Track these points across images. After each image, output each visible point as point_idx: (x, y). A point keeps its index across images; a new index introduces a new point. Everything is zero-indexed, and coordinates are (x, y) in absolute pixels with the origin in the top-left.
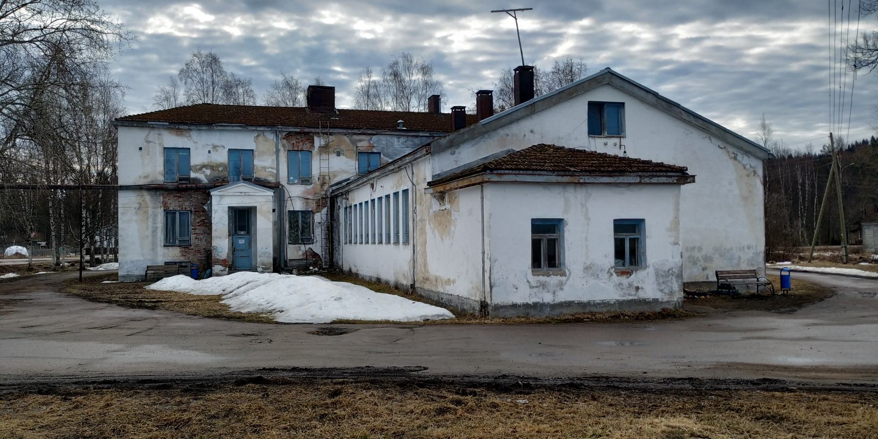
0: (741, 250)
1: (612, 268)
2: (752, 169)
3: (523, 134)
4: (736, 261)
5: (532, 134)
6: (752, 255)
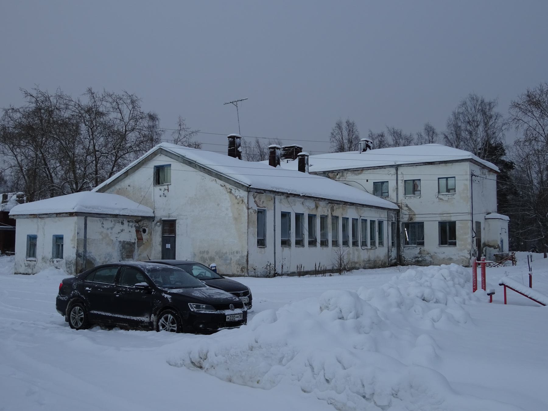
0: (232, 254)
1: (51, 259)
2: (241, 199)
3: (126, 188)
4: (228, 261)
5: (129, 187)
6: (238, 258)
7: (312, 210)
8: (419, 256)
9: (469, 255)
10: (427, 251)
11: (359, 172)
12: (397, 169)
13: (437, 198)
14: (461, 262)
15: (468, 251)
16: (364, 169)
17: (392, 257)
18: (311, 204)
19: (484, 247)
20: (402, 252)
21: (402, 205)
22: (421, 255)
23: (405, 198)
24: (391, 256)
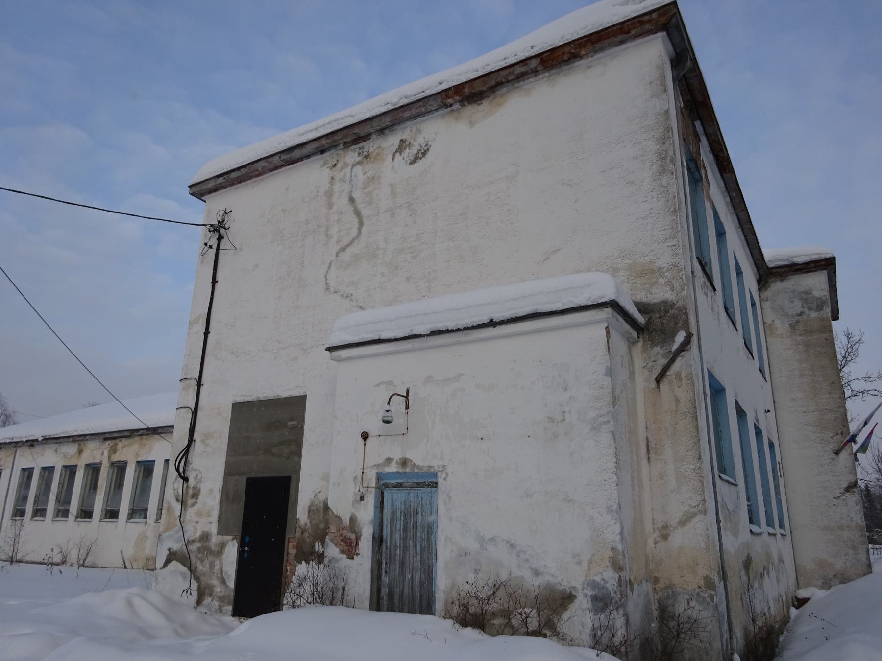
7: (71, 457)
18: (71, 449)
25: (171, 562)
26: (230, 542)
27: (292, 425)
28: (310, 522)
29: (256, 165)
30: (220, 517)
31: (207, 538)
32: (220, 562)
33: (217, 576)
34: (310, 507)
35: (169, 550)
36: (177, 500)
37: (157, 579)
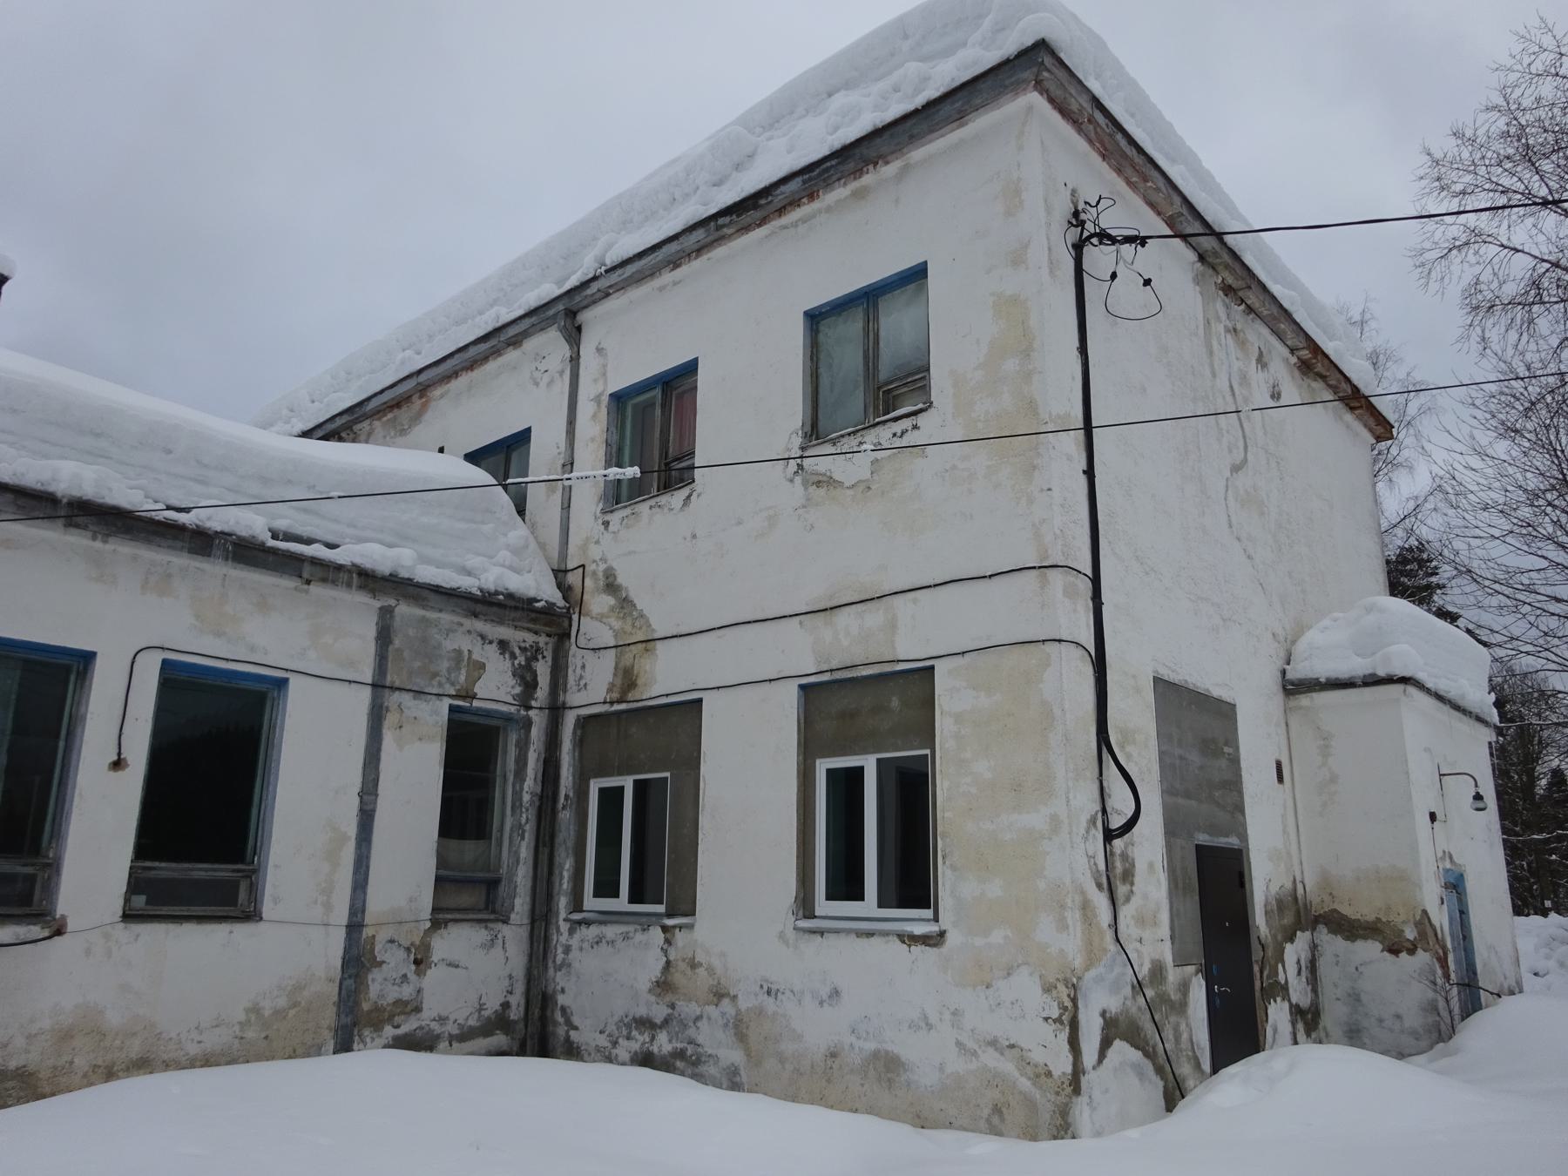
8: (659, 1012)
9: (1064, 1035)
10: (711, 971)
11: (417, 403)
12: (579, 329)
13: (798, 480)
14: (986, 1112)
15: (1048, 989)
16: (423, 378)
17: (428, 1014)
19: (1291, 939)
20: (560, 970)
21: (588, 582)
22: (673, 1006)
23: (606, 524)
24: (418, 1009)
25: (1112, 1044)
26: (1194, 980)
27: (1229, 754)
28: (1270, 931)
29: (1156, 174)
30: (1172, 929)
31: (1161, 974)
32: (1187, 1025)
33: (1187, 1055)
34: (1265, 906)
35: (1103, 1014)
36: (1099, 886)
37: (1090, 1097)
